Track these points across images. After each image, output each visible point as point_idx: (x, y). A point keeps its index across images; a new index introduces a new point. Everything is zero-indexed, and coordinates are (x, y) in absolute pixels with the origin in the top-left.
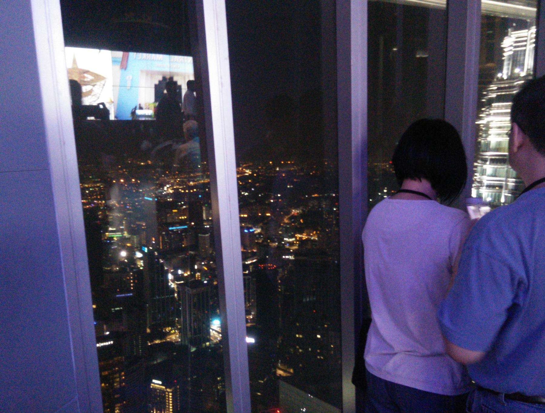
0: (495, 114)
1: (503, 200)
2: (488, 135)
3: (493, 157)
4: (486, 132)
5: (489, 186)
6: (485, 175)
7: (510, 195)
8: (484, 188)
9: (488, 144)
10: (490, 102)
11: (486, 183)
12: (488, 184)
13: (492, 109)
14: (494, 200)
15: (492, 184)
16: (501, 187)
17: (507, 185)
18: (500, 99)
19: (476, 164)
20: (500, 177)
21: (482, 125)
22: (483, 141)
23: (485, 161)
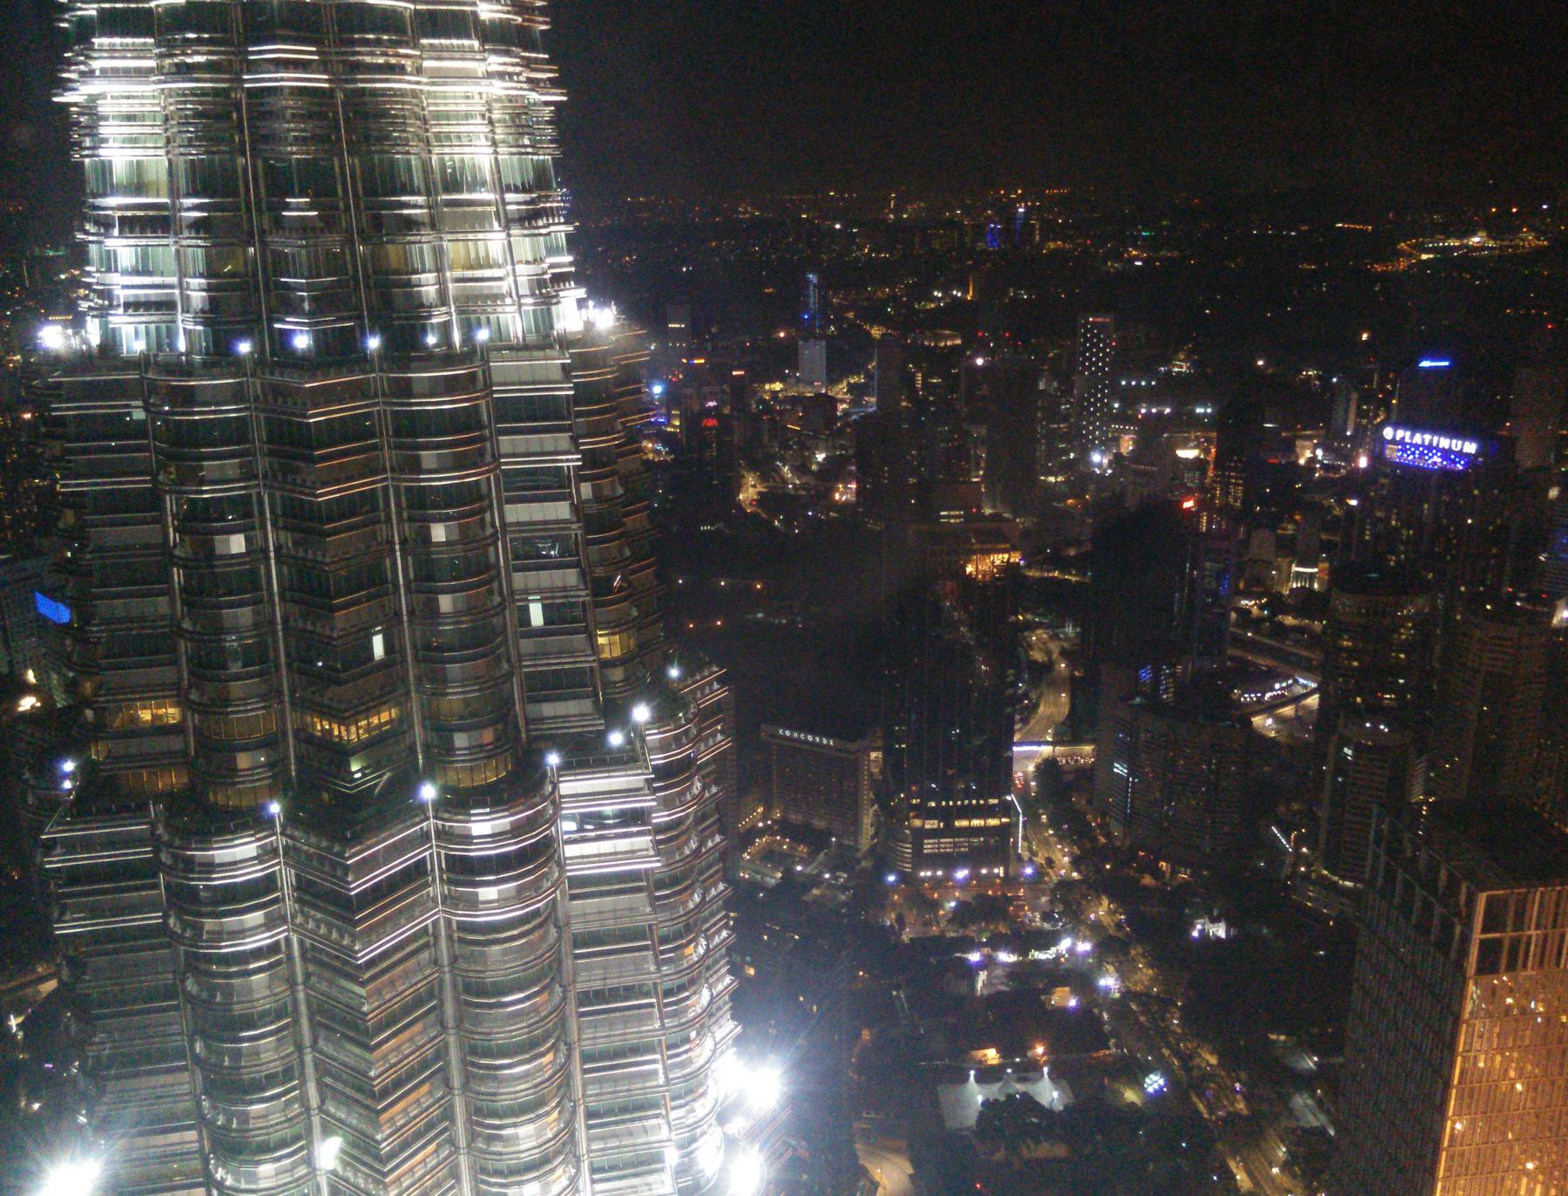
0: (105, 73)
1: (182, 345)
2: (100, 142)
3: (129, 214)
4: (91, 130)
5: (133, 306)
6: (116, 271)
7: (200, 328)
8: (121, 310)
9: (105, 169)
10: (85, 32)
11: (122, 295)
12: (131, 300)
13: (95, 55)
14: (159, 346)
15: (143, 299)
16: (166, 306)
17: (186, 300)
18: (115, 23)
19: (80, 236)
20: (162, 274)
21: (74, 109)
22: (87, 160)
23: (105, 224)
